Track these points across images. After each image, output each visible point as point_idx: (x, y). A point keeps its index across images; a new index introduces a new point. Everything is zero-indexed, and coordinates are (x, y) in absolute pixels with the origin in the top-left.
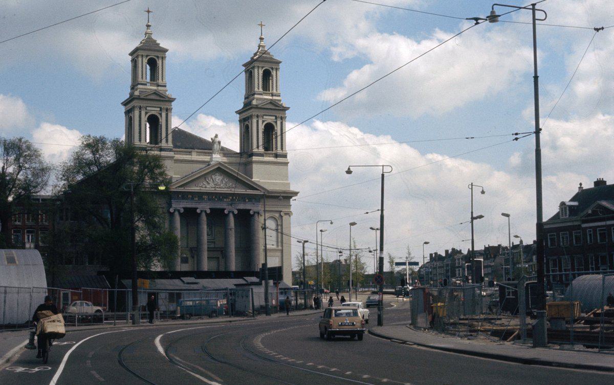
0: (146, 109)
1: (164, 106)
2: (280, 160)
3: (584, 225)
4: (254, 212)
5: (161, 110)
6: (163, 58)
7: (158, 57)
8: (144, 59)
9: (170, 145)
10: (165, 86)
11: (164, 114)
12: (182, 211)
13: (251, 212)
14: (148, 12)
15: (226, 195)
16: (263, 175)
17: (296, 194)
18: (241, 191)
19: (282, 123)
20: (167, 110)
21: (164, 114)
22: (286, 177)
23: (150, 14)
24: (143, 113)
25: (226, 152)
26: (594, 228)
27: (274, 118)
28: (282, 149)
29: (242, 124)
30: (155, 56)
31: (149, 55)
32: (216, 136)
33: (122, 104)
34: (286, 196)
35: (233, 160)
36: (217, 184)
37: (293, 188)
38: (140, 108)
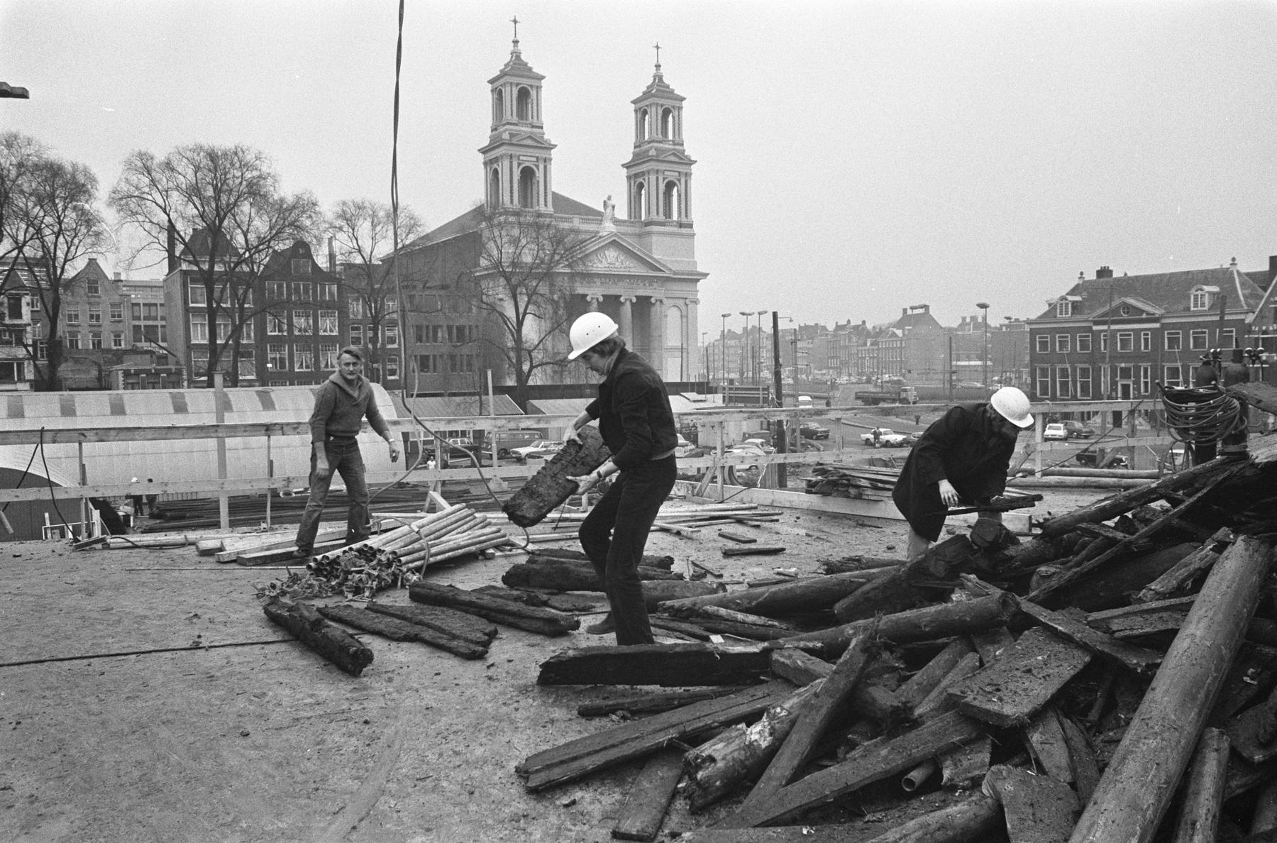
1: (542, 154)
2: (684, 230)
3: (1095, 328)
6: (539, 88)
9: (550, 209)
11: (541, 167)
13: (653, 300)
15: (621, 277)
16: (662, 250)
17: (706, 275)
18: (642, 271)
20: (545, 160)
21: (541, 167)
22: (691, 252)
24: (515, 164)
25: (617, 222)
26: (1137, 332)
32: (609, 198)
34: (693, 278)
35: (623, 229)
36: (610, 261)
37: (699, 269)
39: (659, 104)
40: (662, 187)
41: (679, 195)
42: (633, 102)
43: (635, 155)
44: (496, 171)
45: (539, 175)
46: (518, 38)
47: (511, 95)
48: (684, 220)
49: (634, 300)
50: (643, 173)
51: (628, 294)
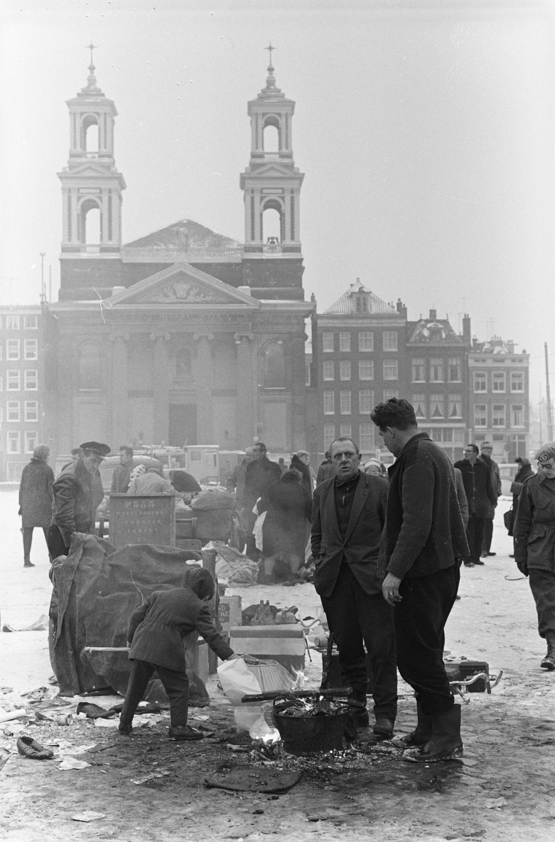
5: (101, 192)
8: (78, 118)
11: (105, 198)
12: (127, 337)
19: (292, 199)
23: (273, 51)
27: (280, 191)
28: (292, 238)
31: (86, 113)
38: (110, 191)
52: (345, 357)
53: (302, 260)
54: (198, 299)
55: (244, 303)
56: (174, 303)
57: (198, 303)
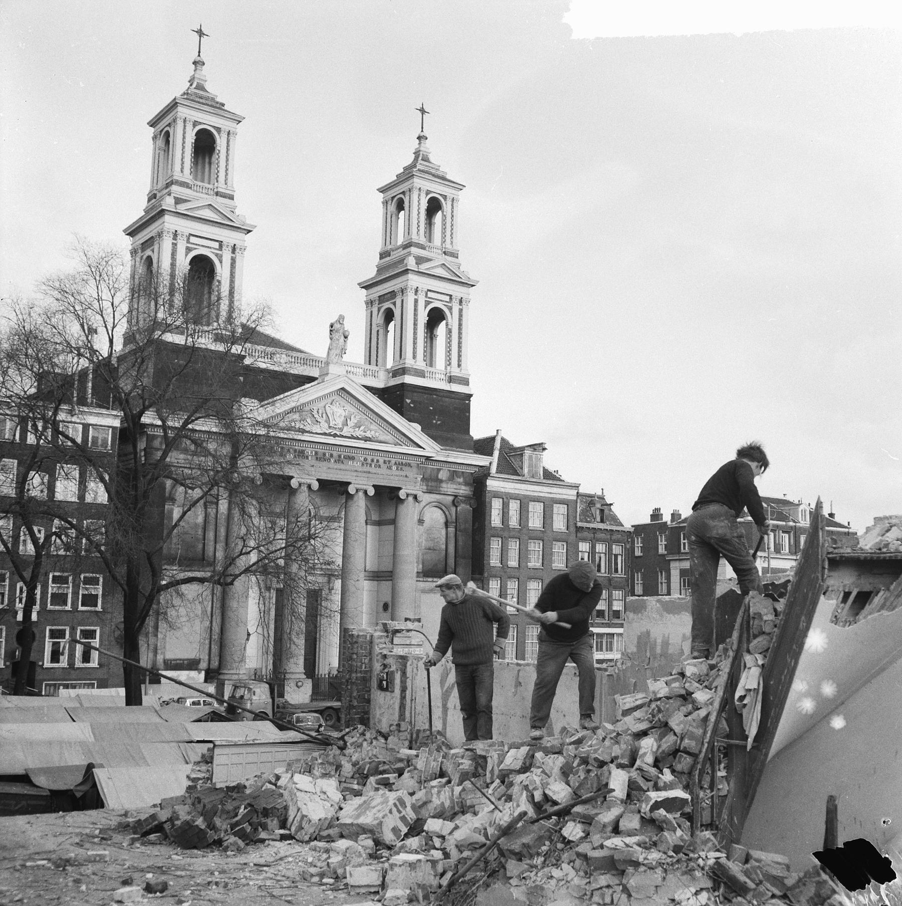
0: (188, 242)
4: (408, 495)
7: (219, 130)
10: (231, 198)
14: (200, 33)
28: (459, 366)
29: (375, 310)
30: (214, 127)
33: (125, 231)
39: (417, 197)
40: (423, 318)
41: (449, 331)
42: (382, 190)
43: (380, 270)
44: (149, 260)
45: (222, 272)
46: (203, 57)
47: (184, 142)
48: (455, 371)
49: (371, 492)
50: (392, 295)
51: (362, 482)
52: (535, 536)
53: (469, 396)
54: (358, 433)
55: (421, 447)
56: (325, 434)
57: (358, 438)
